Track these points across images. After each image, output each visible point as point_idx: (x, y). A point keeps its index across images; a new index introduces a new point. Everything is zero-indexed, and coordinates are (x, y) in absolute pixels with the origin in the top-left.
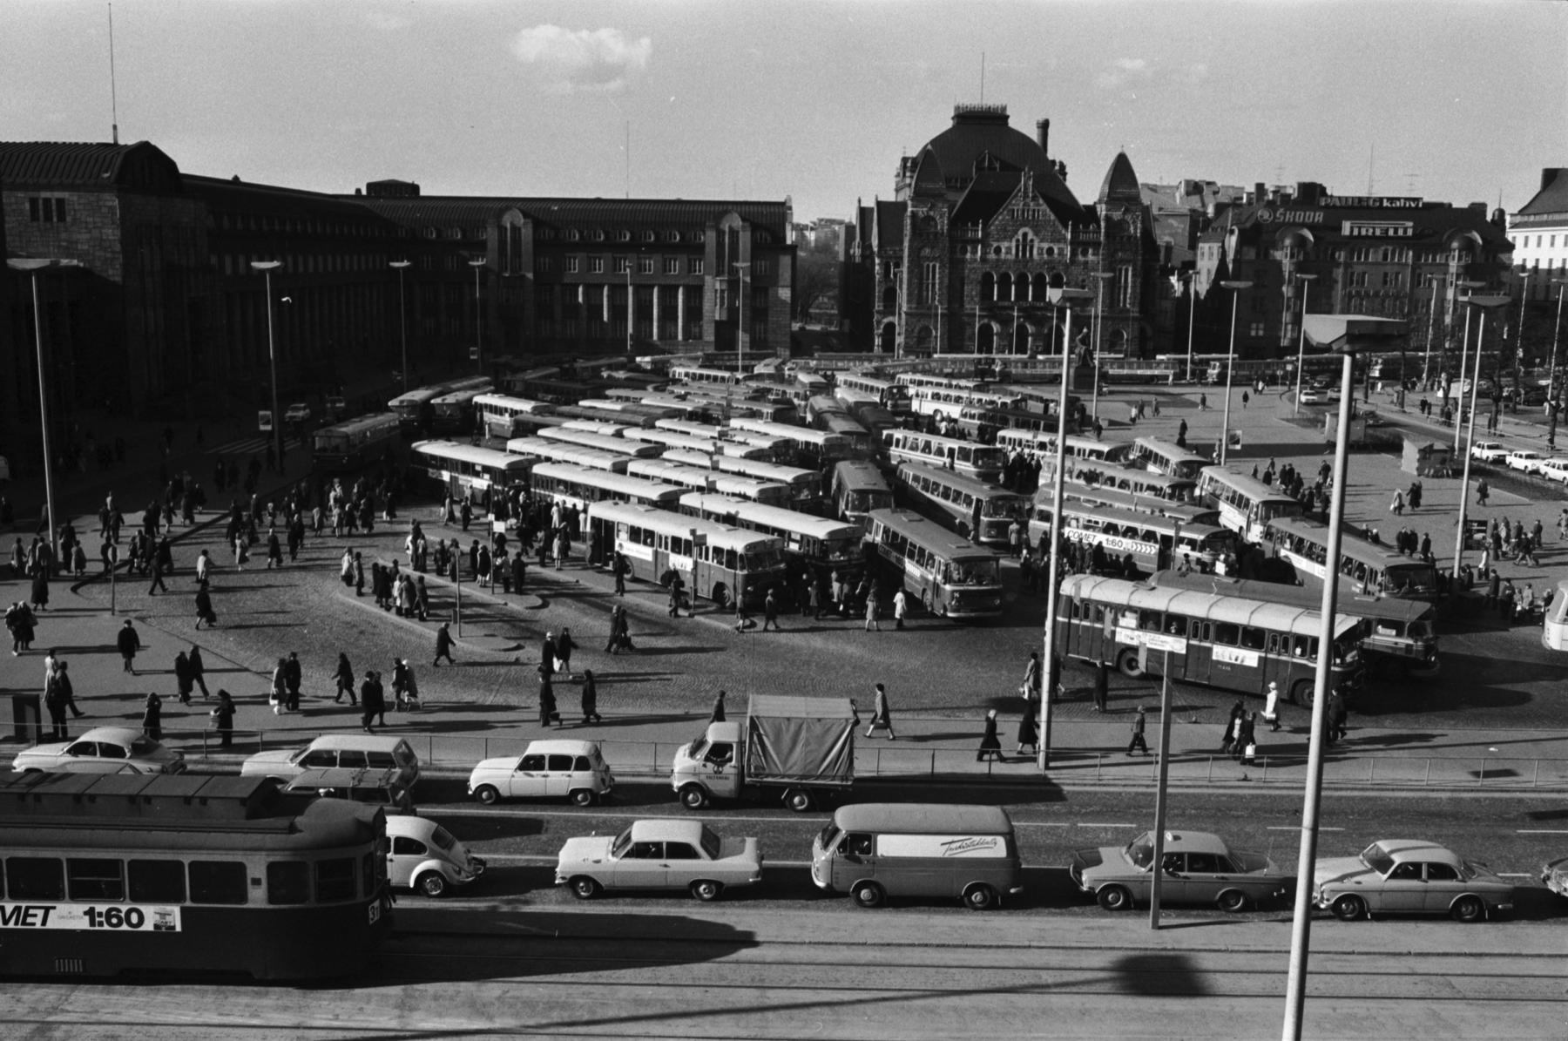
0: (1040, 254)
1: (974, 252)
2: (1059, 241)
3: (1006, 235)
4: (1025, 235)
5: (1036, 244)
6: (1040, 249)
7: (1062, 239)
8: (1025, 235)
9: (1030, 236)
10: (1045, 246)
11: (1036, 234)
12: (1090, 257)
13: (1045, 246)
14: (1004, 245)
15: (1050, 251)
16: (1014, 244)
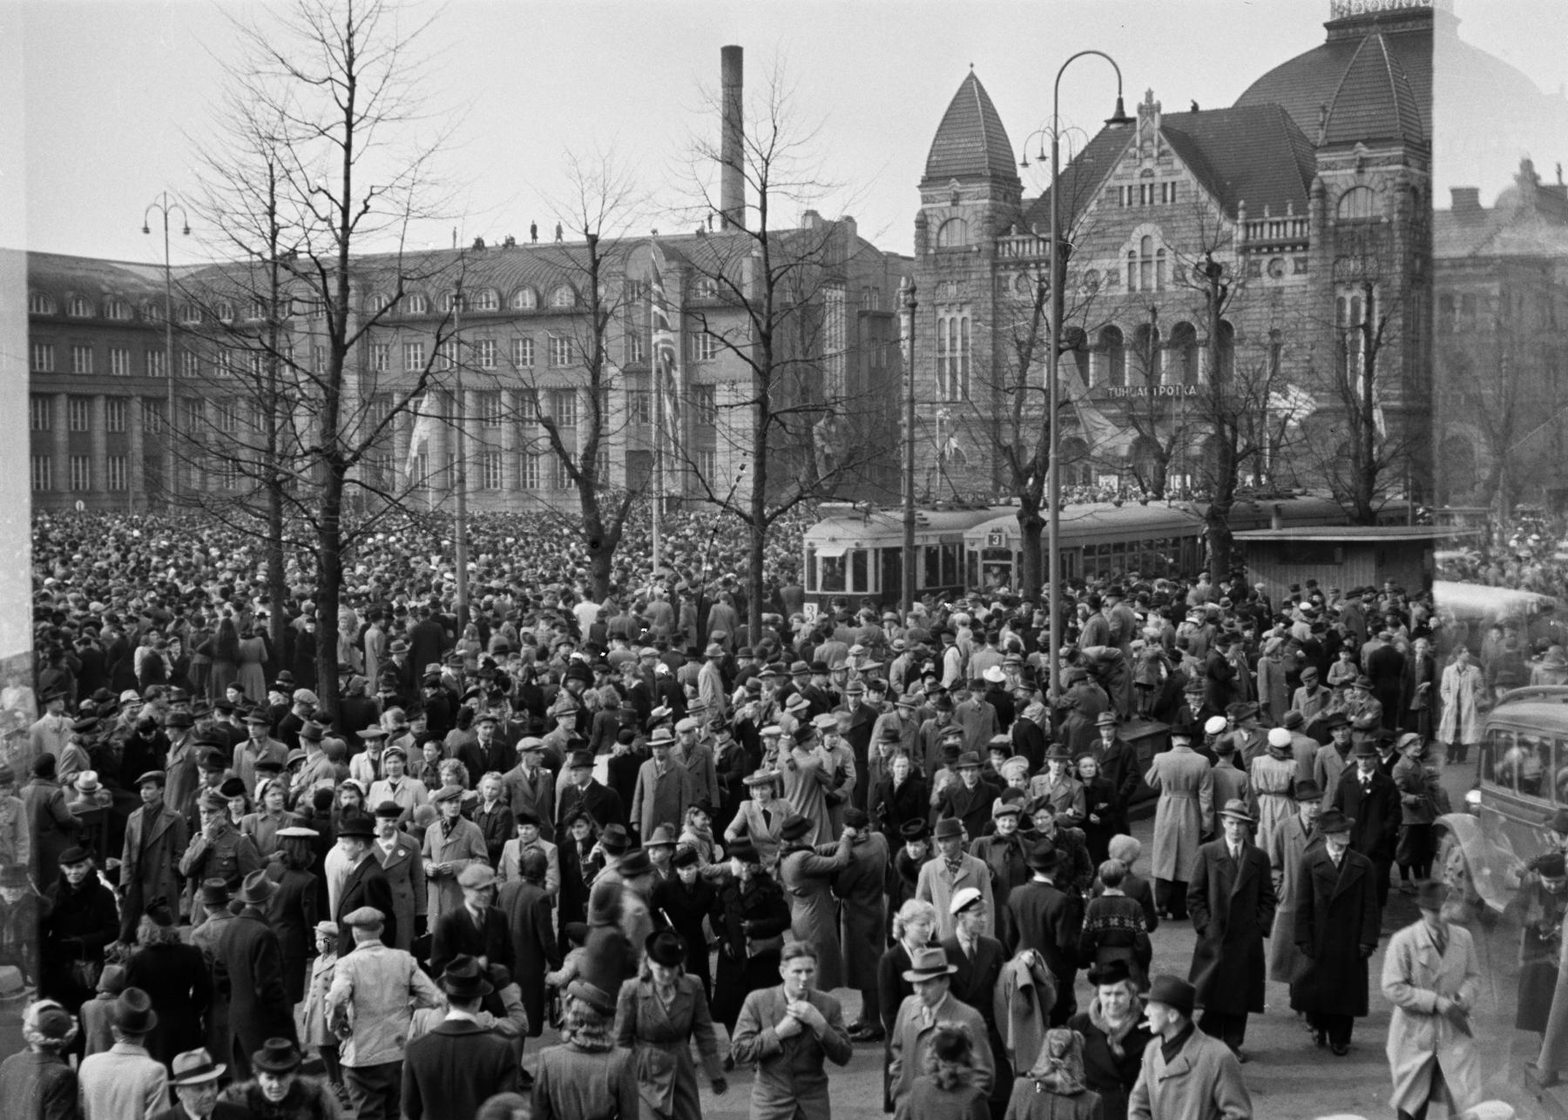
9: (1157, 244)
16: (1125, 261)
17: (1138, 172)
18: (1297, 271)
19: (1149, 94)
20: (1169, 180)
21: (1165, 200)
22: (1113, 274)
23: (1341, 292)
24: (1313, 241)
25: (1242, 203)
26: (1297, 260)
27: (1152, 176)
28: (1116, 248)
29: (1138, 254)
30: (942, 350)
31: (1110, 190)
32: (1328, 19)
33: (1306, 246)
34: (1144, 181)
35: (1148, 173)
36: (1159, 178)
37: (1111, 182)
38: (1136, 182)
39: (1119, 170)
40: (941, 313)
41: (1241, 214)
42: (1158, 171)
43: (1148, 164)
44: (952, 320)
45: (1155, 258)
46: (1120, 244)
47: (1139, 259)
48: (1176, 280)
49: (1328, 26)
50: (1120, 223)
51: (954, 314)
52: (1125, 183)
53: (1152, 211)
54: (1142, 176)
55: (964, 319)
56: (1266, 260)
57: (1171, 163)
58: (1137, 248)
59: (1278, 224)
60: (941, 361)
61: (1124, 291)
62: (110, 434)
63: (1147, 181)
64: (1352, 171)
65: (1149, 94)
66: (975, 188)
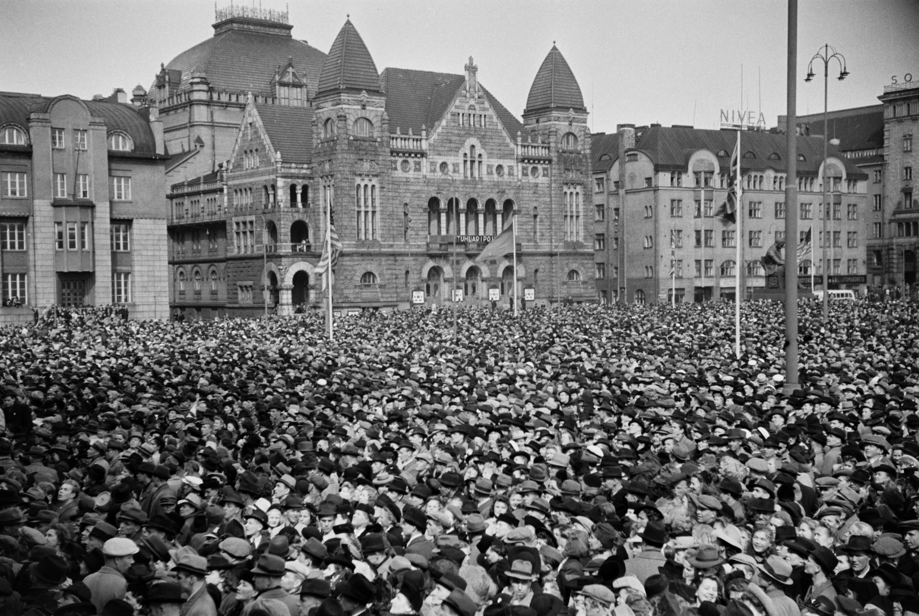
0: (490, 173)
1: (418, 169)
2: (503, 157)
3: (450, 144)
5: (485, 159)
6: (489, 166)
7: (509, 155)
8: (473, 146)
9: (479, 150)
10: (495, 162)
11: (484, 145)
12: (542, 180)
13: (495, 162)
14: (450, 160)
15: (500, 167)
16: (461, 159)
17: (467, 106)
18: (544, 175)
19: (471, 59)
20: (483, 113)
22: (456, 165)
23: (565, 189)
24: (555, 159)
25: (519, 133)
26: (545, 169)
28: (457, 150)
29: (469, 155)
30: (359, 206)
31: (453, 115)
32: (214, 22)
33: (550, 161)
34: (471, 112)
35: (472, 107)
36: (478, 112)
37: (452, 109)
38: (466, 112)
39: (457, 103)
40: (358, 180)
41: (519, 139)
42: (477, 107)
43: (472, 102)
44: (366, 186)
45: (477, 159)
46: (459, 148)
47: (469, 159)
48: (488, 174)
49: (215, 26)
50: (459, 135)
51: (366, 181)
52: (461, 112)
54: (469, 109)
55: (373, 186)
56: (400, 160)
57: (483, 103)
58: (468, 152)
60: (359, 212)
61: (462, 178)
62: (14, 239)
63: (472, 112)
64: (567, 123)
65: (471, 59)
66: (376, 99)
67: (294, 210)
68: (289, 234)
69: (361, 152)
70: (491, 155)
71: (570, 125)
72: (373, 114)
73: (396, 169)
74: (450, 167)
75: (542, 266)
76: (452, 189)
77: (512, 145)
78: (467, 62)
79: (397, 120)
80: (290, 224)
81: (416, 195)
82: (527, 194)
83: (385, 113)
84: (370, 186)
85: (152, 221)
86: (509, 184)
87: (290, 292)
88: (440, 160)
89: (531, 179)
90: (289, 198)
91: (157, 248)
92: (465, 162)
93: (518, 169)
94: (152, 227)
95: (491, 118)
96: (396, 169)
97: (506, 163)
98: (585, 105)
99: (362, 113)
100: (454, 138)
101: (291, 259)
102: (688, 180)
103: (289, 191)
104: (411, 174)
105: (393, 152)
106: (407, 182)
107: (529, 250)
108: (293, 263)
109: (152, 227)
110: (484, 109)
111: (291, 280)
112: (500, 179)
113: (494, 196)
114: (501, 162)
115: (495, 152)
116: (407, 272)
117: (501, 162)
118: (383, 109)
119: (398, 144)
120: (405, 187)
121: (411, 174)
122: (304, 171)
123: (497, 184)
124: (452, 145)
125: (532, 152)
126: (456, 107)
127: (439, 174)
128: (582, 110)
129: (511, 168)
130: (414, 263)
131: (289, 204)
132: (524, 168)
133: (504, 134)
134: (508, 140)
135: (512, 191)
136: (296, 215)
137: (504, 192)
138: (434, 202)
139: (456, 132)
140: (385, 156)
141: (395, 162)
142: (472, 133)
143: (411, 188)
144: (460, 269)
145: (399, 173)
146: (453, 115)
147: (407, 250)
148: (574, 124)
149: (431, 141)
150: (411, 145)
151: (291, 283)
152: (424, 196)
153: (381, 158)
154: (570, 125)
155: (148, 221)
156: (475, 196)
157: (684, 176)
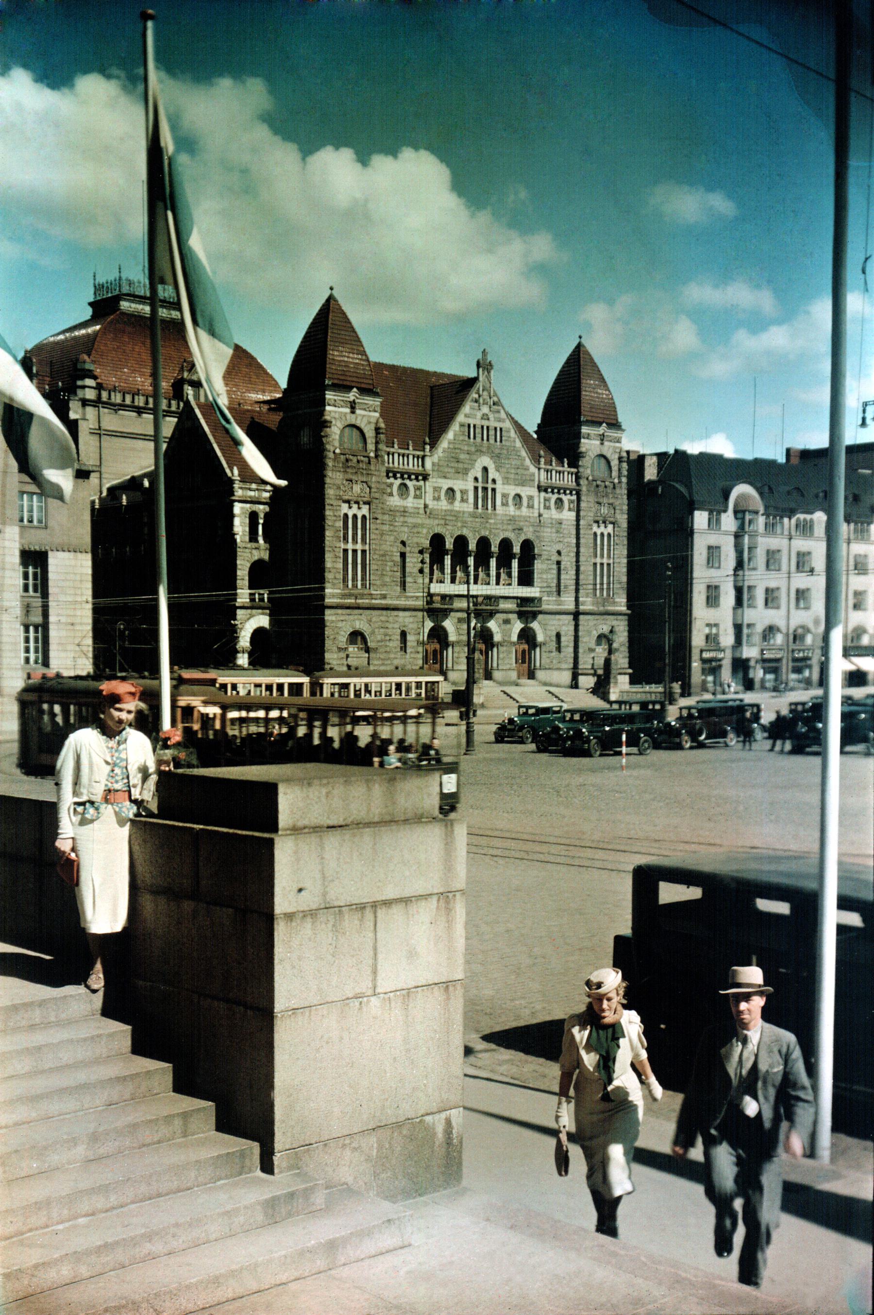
2: (522, 484)
4: (485, 470)
6: (505, 496)
8: (485, 470)
9: (492, 473)
13: (512, 490)
16: (470, 485)
17: (479, 415)
21: (496, 441)
27: (488, 419)
28: (466, 472)
29: (480, 480)
31: (462, 425)
35: (485, 417)
36: (493, 424)
42: (491, 416)
52: (472, 422)
53: (489, 448)
58: (480, 476)
59: (560, 472)
66: (369, 401)
67: (254, 545)
68: (247, 578)
69: (349, 470)
70: (506, 480)
71: (602, 444)
72: (365, 420)
73: (391, 494)
74: (458, 495)
75: (564, 628)
76: (459, 524)
77: (533, 469)
78: (480, 357)
79: (393, 431)
80: (249, 565)
81: (415, 530)
82: (548, 533)
83: (381, 420)
84: (350, 516)
85: (72, 555)
86: (526, 519)
87: (246, 655)
88: (445, 484)
89: (554, 514)
90: (247, 529)
91: (79, 592)
92: (476, 488)
93: (539, 499)
94: (73, 563)
95: (508, 431)
96: (391, 494)
97: (527, 491)
98: (620, 420)
99: (351, 419)
100: (462, 456)
101: (249, 611)
102: (728, 521)
103: (247, 521)
104: (410, 502)
105: (391, 473)
106: (404, 512)
107: (550, 607)
108: (251, 616)
109: (73, 563)
110: (500, 420)
111: (248, 640)
112: (518, 513)
113: (511, 536)
114: (518, 490)
115: (512, 476)
116: (404, 634)
117: (518, 490)
118: (377, 415)
119: (397, 463)
120: (402, 519)
121: (410, 502)
122: (252, 493)
123: (512, 519)
124: (461, 465)
125: (555, 480)
126: (466, 416)
127: (444, 504)
128: (615, 425)
129: (530, 498)
130: (411, 620)
131: (247, 538)
132: (545, 500)
133: (523, 453)
134: (528, 462)
135: (531, 529)
136: (255, 552)
137: (521, 529)
138: (437, 540)
139: (466, 448)
140: (378, 476)
141: (391, 485)
142: (484, 449)
143: (410, 520)
144: (511, 630)
145: (395, 501)
146: (462, 425)
147: (402, 602)
148: (606, 443)
149: (435, 458)
150: (412, 465)
151: (248, 644)
152: (425, 531)
153: (374, 479)
154: (602, 444)
155: (66, 554)
156: (438, 530)
157: (724, 516)
